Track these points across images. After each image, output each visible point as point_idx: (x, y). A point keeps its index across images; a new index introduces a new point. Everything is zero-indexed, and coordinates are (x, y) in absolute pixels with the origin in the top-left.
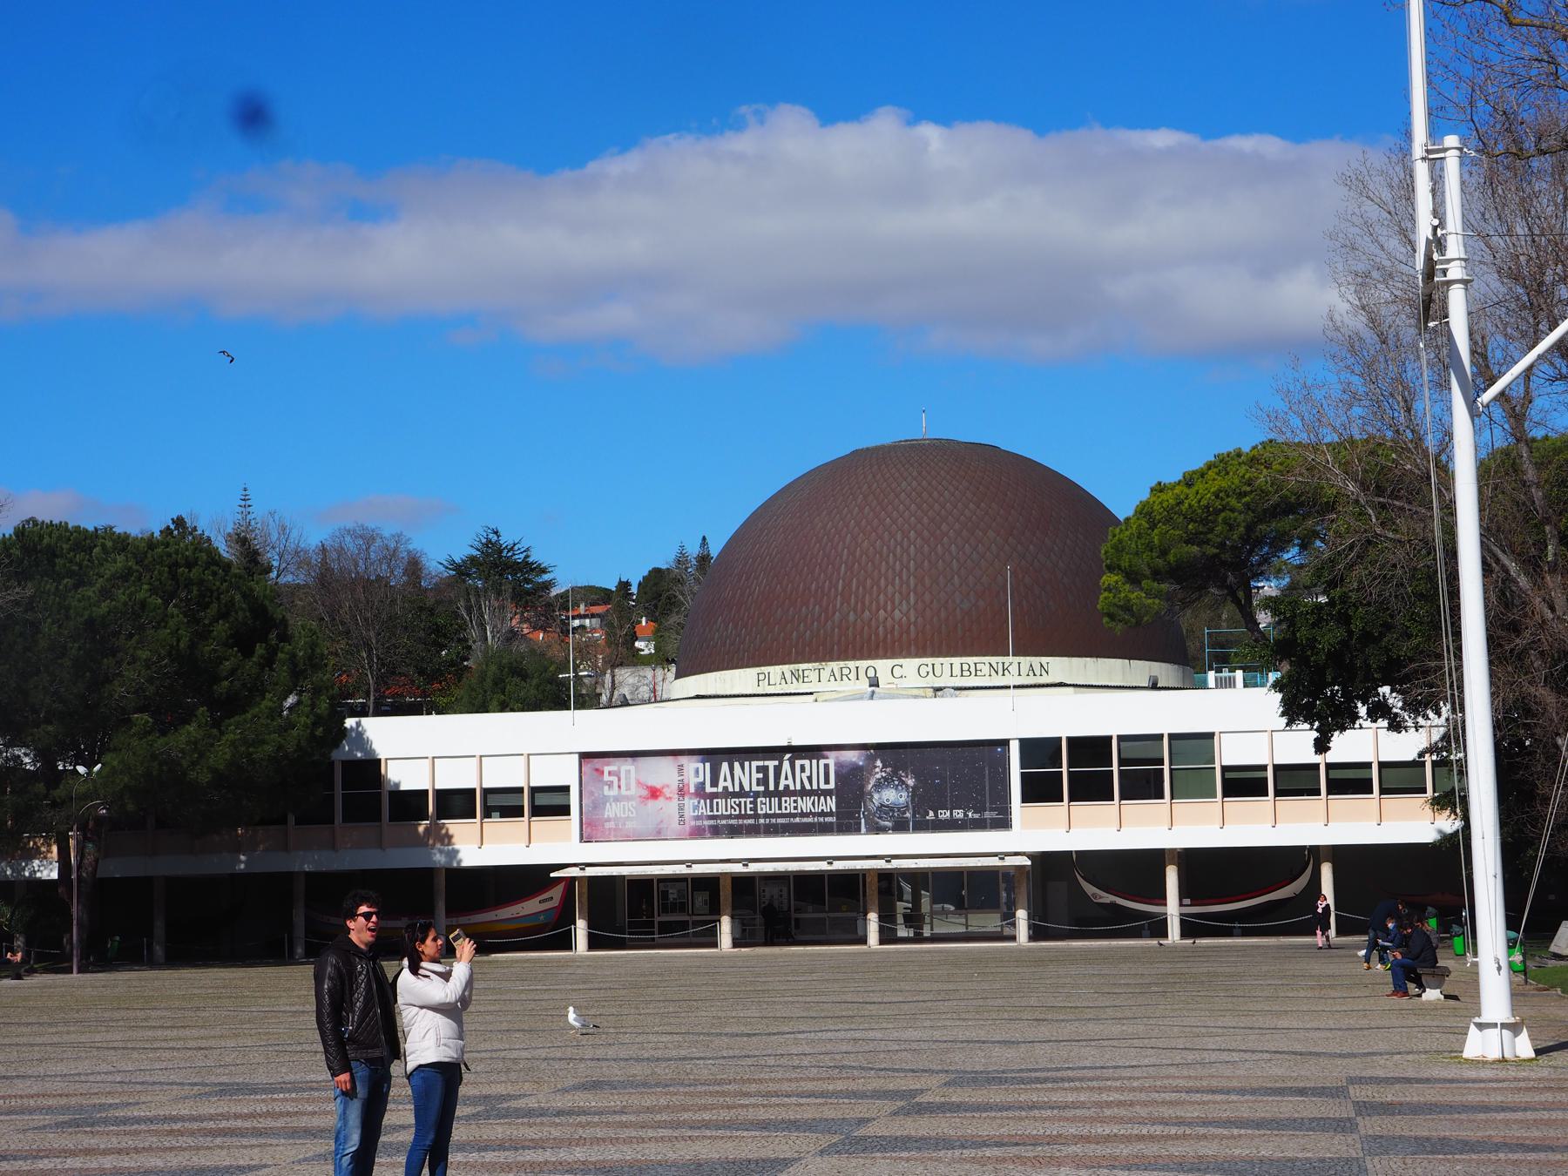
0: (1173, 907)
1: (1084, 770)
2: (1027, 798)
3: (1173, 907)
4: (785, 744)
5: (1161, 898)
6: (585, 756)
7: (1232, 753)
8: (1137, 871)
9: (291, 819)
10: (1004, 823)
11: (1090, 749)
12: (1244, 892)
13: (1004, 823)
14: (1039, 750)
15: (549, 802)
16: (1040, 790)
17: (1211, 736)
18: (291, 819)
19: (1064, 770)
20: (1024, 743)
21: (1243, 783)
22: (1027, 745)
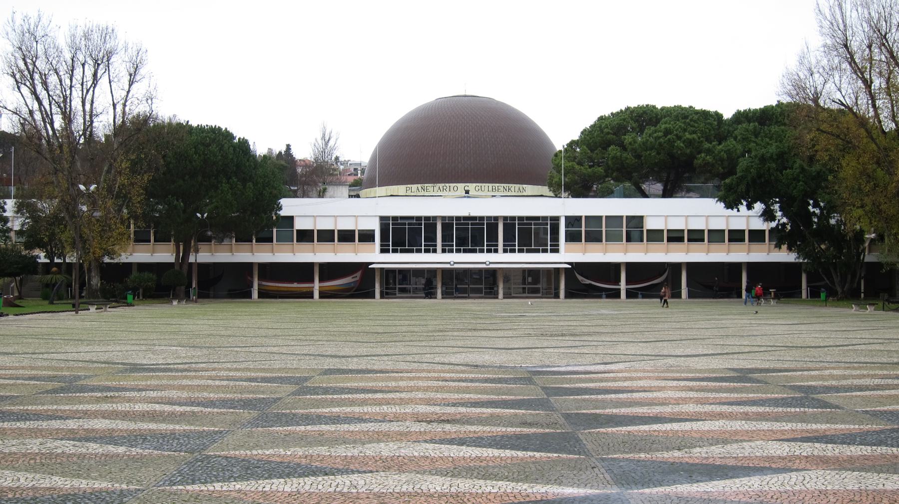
0: (623, 285)
3: (623, 285)
4: (467, 214)
5: (617, 281)
6: (382, 218)
7: (650, 224)
8: (609, 271)
9: (254, 241)
10: (555, 250)
13: (555, 250)
14: (573, 221)
15: (367, 237)
16: (573, 237)
17: (642, 217)
18: (254, 241)
19: (583, 229)
20: (567, 218)
21: (655, 236)
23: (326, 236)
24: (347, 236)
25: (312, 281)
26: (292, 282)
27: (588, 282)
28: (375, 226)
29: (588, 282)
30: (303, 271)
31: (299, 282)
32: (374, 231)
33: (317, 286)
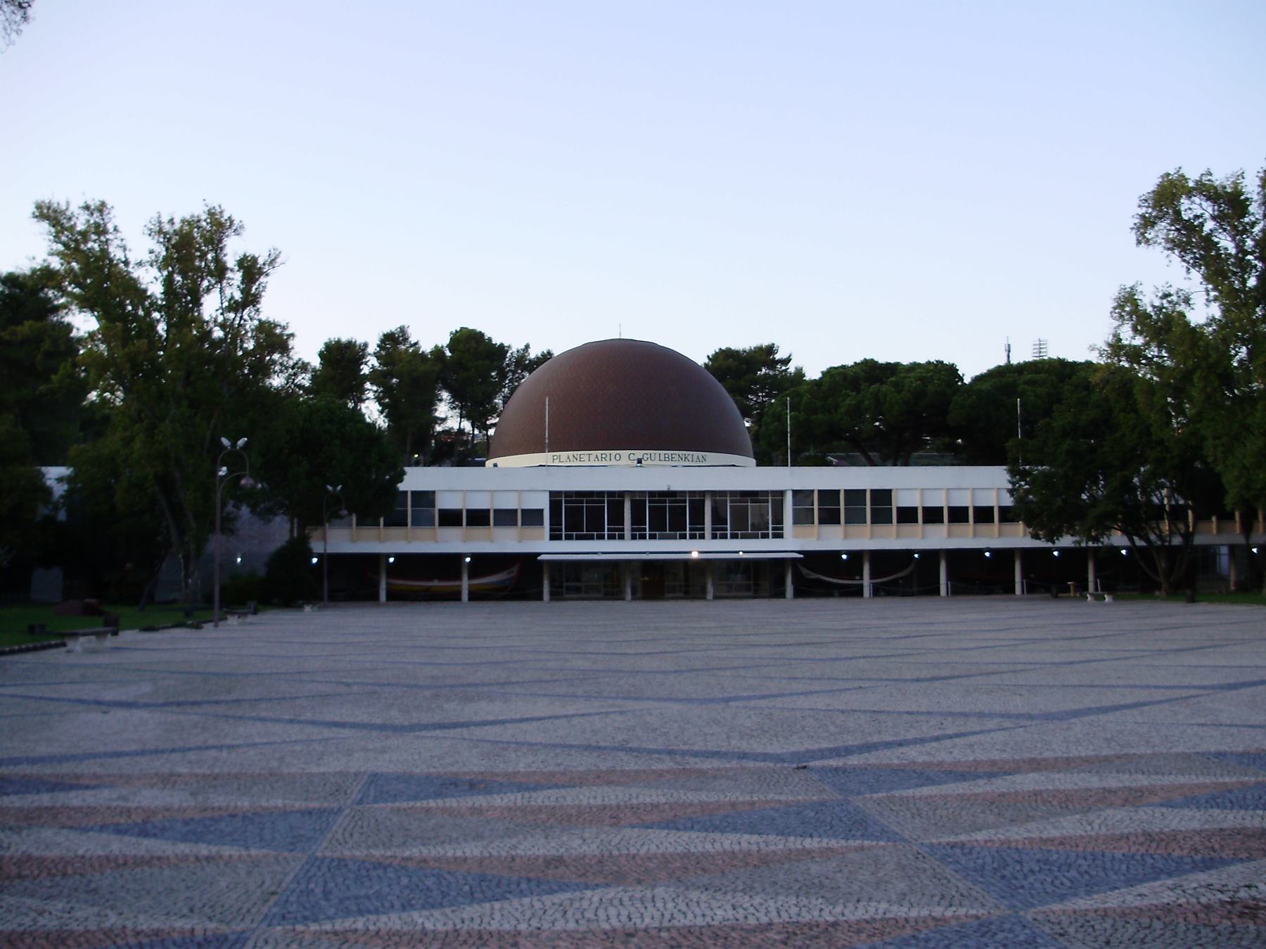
0: (866, 581)
1: (829, 508)
2: (797, 521)
3: (866, 581)
4: (665, 489)
6: (552, 494)
7: (902, 500)
11: (829, 496)
12: (905, 576)
15: (532, 517)
16: (802, 518)
21: (908, 515)
22: (795, 492)
23: (478, 518)
24: (506, 517)
25: (459, 578)
26: (431, 579)
27: (814, 576)
28: (543, 503)
29: (814, 576)
30: (448, 564)
31: (441, 579)
32: (542, 511)
33: (465, 584)
